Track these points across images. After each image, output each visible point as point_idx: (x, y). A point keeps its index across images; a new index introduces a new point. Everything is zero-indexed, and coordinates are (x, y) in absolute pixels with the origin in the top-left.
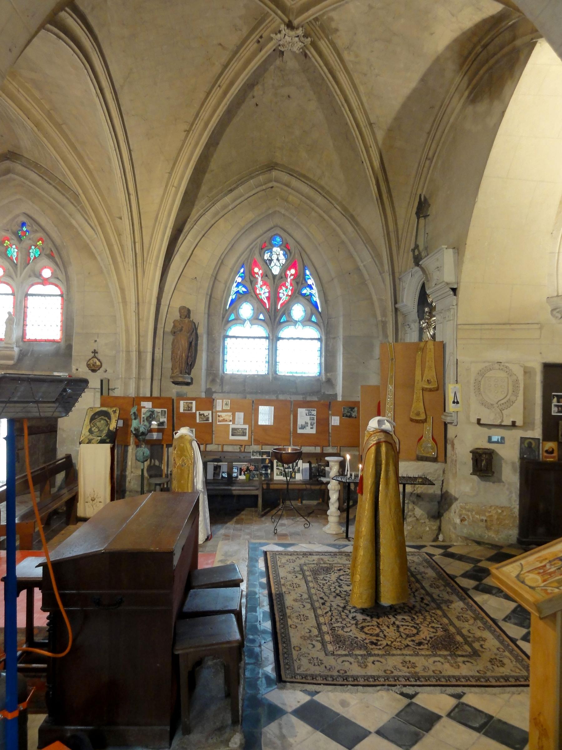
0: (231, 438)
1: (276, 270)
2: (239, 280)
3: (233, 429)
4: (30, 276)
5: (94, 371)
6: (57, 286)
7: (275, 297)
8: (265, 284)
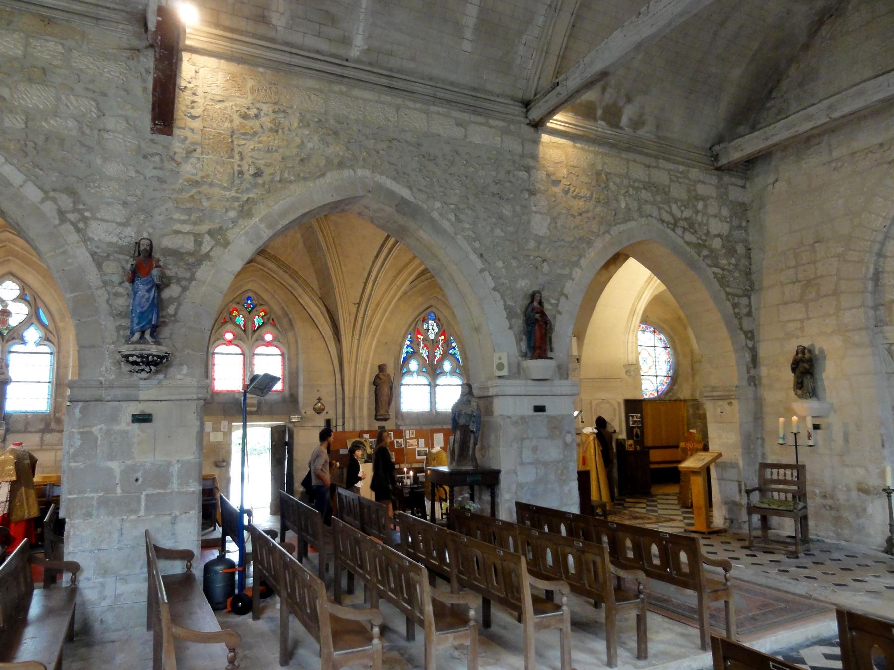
0: (418, 457)
1: (432, 337)
2: (408, 343)
3: (418, 451)
4: (257, 340)
5: (319, 413)
6: (277, 347)
7: (431, 356)
8: (425, 346)
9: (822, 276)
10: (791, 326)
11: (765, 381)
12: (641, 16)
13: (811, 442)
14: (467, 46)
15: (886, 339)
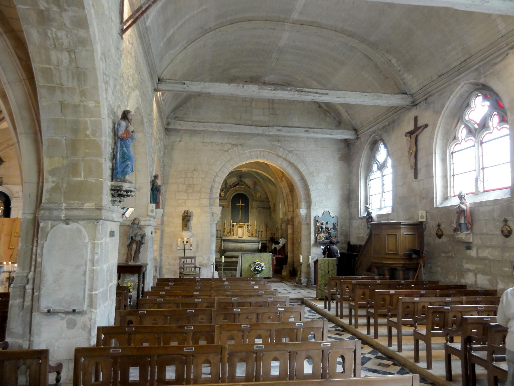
9: (195, 184)
10: (180, 202)
11: (165, 223)
12: (239, 87)
13: (191, 248)
14: (162, 44)
15: (212, 211)
